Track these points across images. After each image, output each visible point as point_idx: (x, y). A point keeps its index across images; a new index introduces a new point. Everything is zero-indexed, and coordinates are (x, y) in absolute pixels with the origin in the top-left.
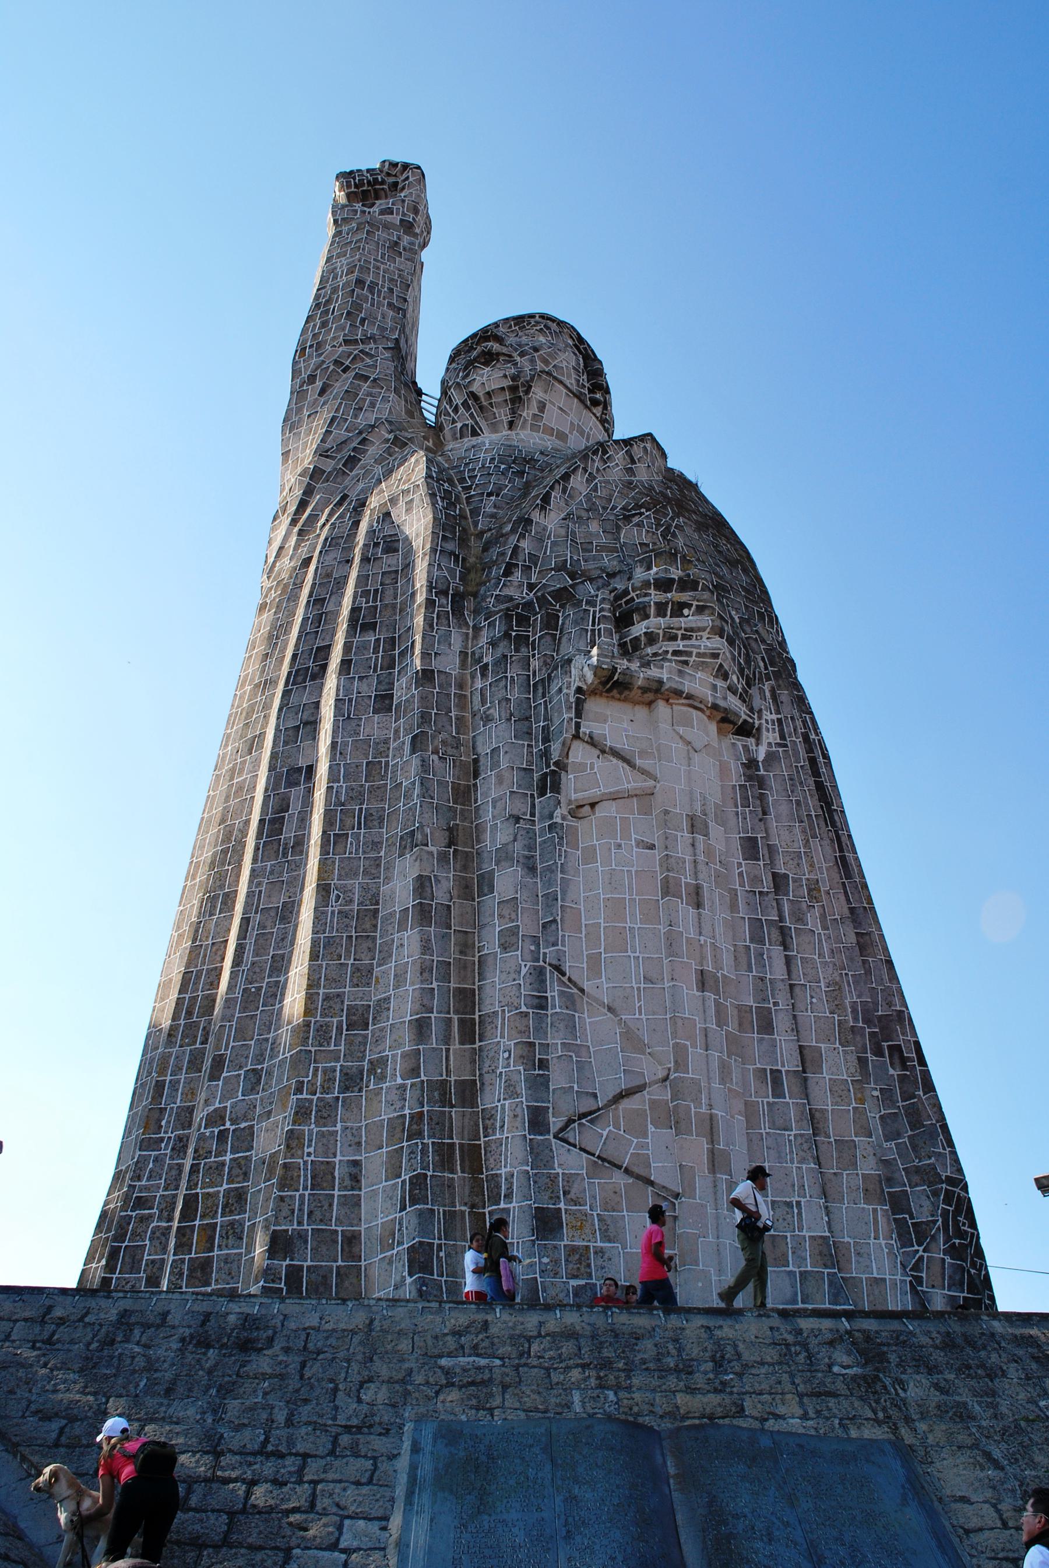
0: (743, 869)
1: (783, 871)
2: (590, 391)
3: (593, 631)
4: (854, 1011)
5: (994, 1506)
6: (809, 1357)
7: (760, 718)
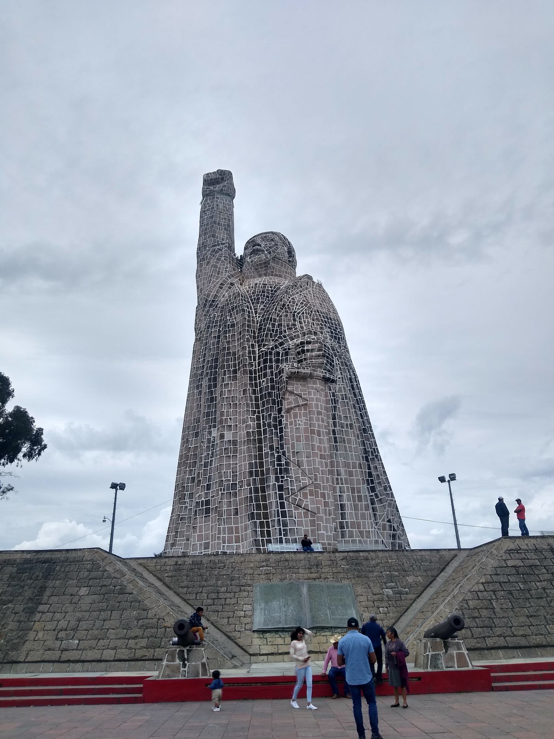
2: (288, 258)
3: (290, 358)
5: (367, 596)
6: (337, 563)
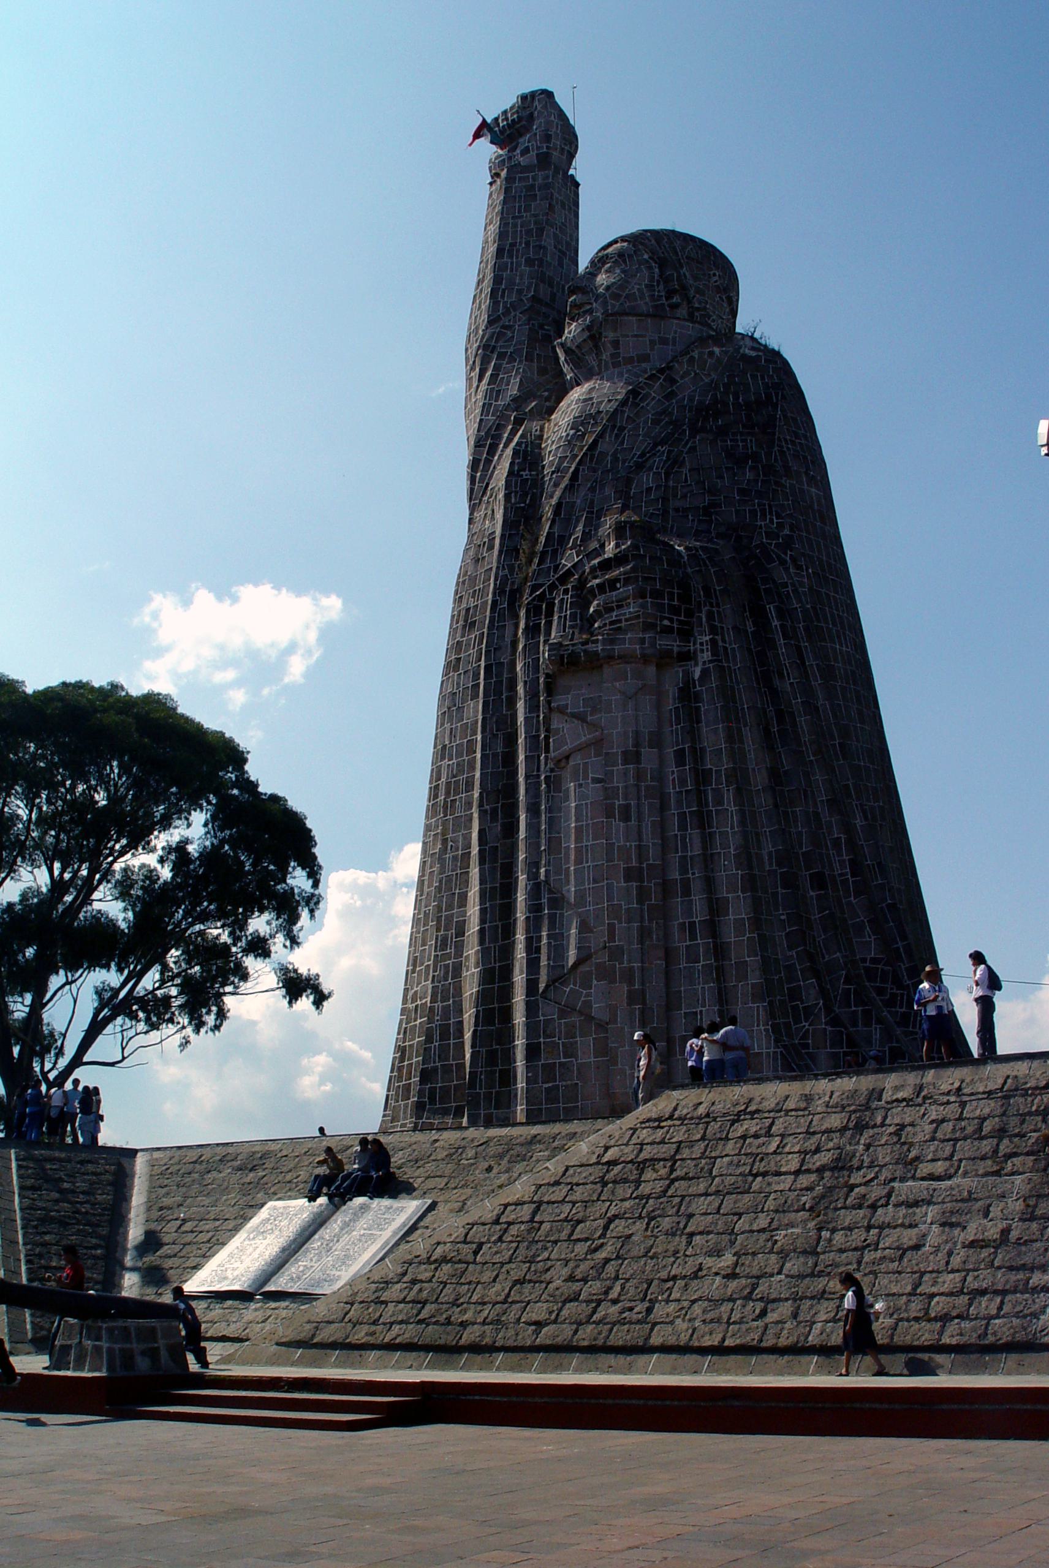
0: (675, 775)
1: (709, 767)
4: (770, 858)
7: (695, 644)
